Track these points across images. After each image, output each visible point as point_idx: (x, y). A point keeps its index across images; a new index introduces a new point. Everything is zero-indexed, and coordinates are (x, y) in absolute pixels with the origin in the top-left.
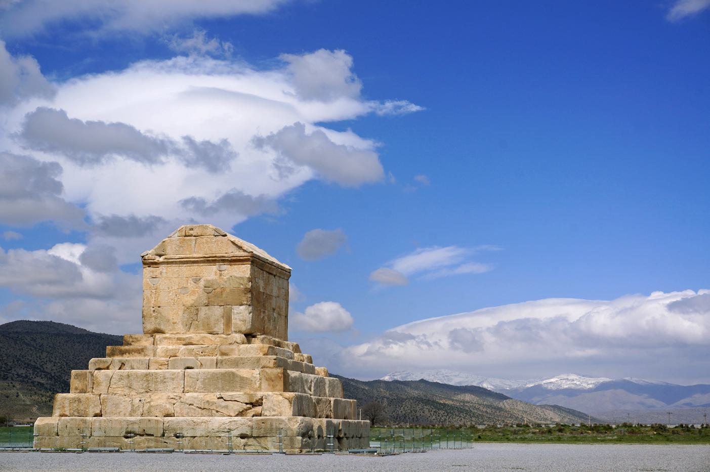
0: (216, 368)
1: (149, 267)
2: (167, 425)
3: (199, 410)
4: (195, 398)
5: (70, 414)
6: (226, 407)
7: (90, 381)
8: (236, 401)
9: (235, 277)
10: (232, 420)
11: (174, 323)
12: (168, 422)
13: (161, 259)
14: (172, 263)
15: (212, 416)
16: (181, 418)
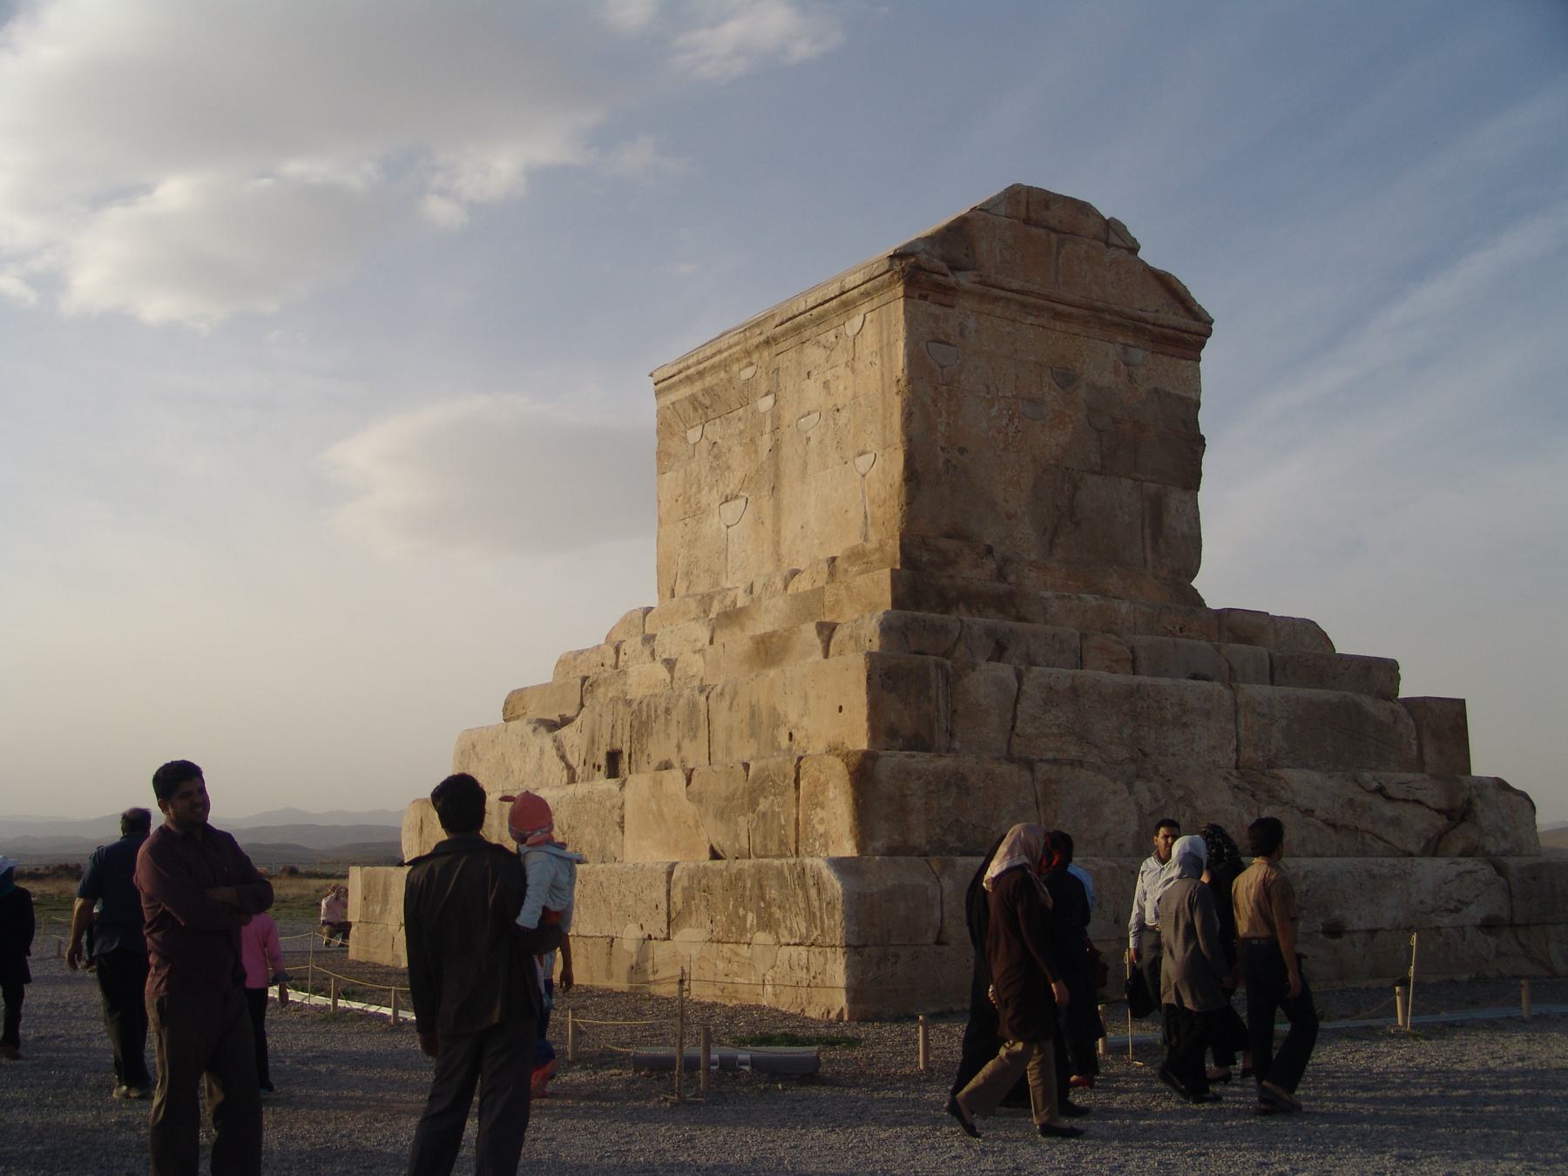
0: (1272, 683)
1: (924, 297)
2: (1304, 888)
3: (1330, 831)
4: (1317, 788)
5: (928, 842)
6: (1396, 822)
7: (942, 703)
8: (1418, 802)
9: (1169, 395)
10: (1461, 868)
11: (1010, 516)
12: (1305, 877)
13: (965, 279)
14: (996, 299)
15: (1365, 854)
16: (1337, 863)
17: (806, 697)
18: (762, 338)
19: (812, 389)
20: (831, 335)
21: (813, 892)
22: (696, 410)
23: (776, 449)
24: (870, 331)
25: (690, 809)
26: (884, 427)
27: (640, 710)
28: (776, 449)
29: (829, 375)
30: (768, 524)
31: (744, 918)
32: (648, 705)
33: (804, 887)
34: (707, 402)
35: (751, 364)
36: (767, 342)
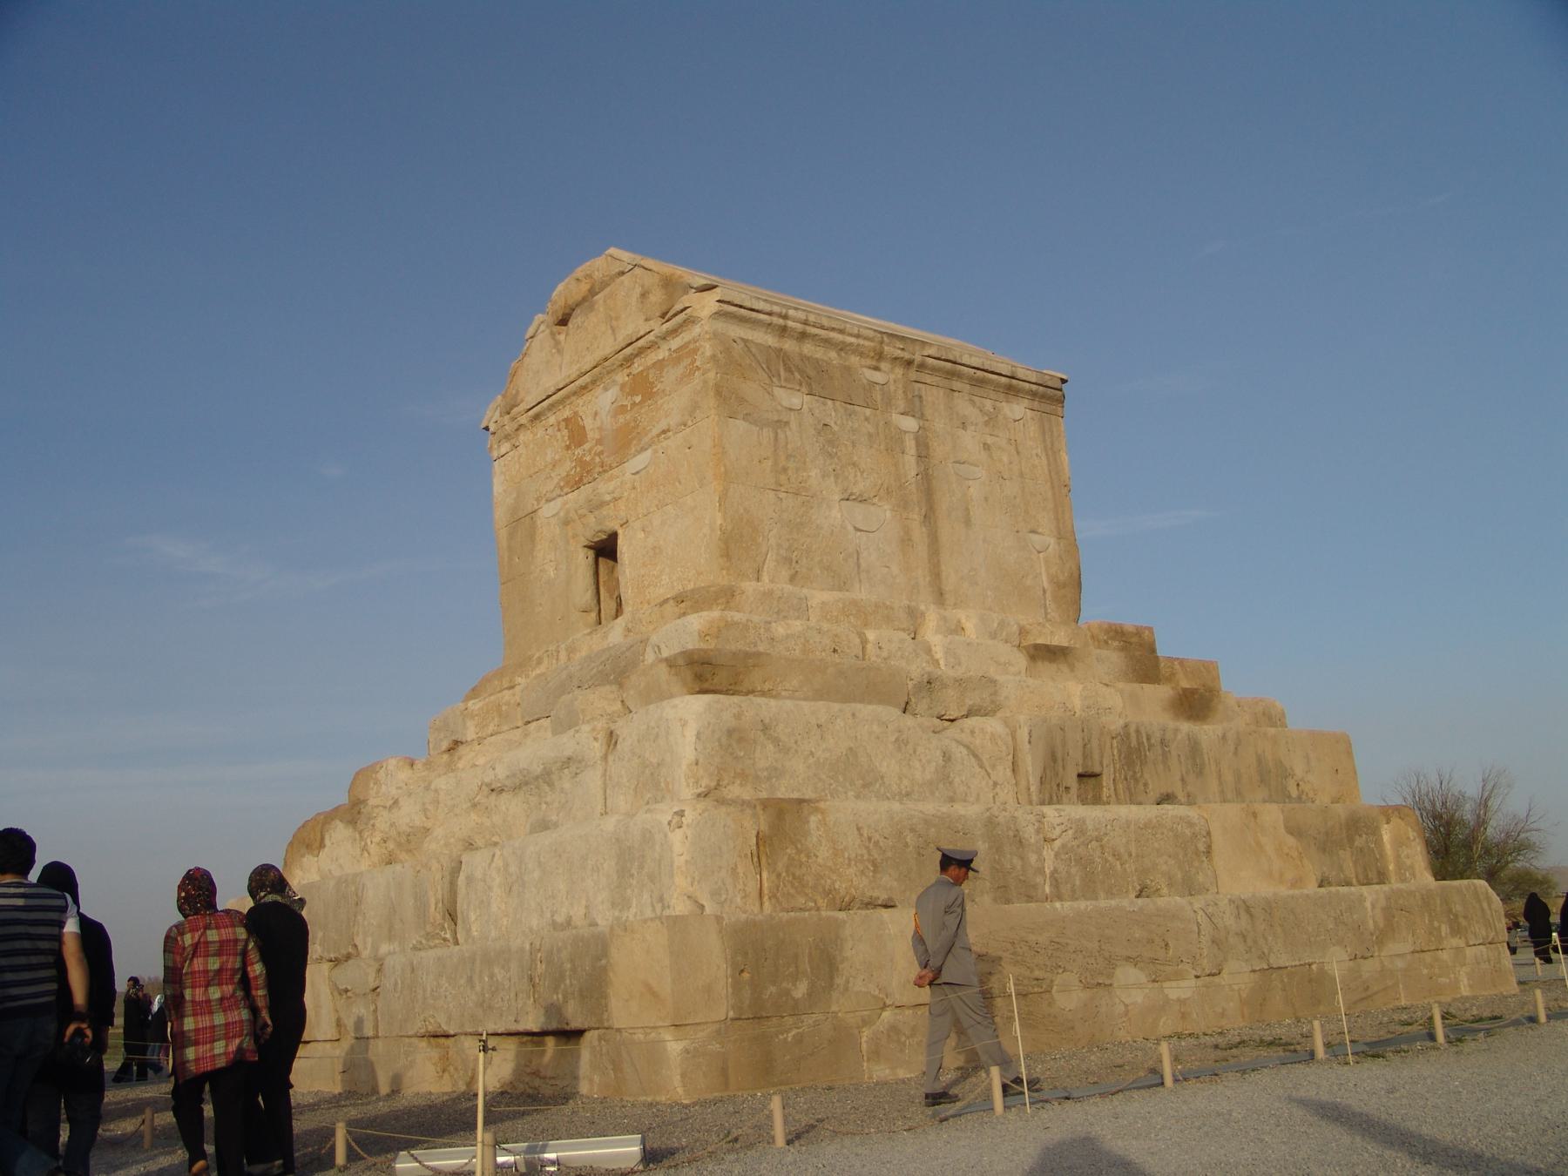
17: (1307, 757)
18: (907, 356)
19: (969, 441)
20: (988, 404)
21: (1485, 905)
22: (788, 370)
23: (926, 477)
24: (1033, 429)
25: (1291, 841)
26: (1057, 519)
27: (1128, 735)
28: (926, 477)
29: (989, 440)
30: (922, 549)
31: (1439, 929)
32: (1138, 731)
33: (1479, 901)
34: (812, 373)
35: (877, 369)
36: (909, 363)
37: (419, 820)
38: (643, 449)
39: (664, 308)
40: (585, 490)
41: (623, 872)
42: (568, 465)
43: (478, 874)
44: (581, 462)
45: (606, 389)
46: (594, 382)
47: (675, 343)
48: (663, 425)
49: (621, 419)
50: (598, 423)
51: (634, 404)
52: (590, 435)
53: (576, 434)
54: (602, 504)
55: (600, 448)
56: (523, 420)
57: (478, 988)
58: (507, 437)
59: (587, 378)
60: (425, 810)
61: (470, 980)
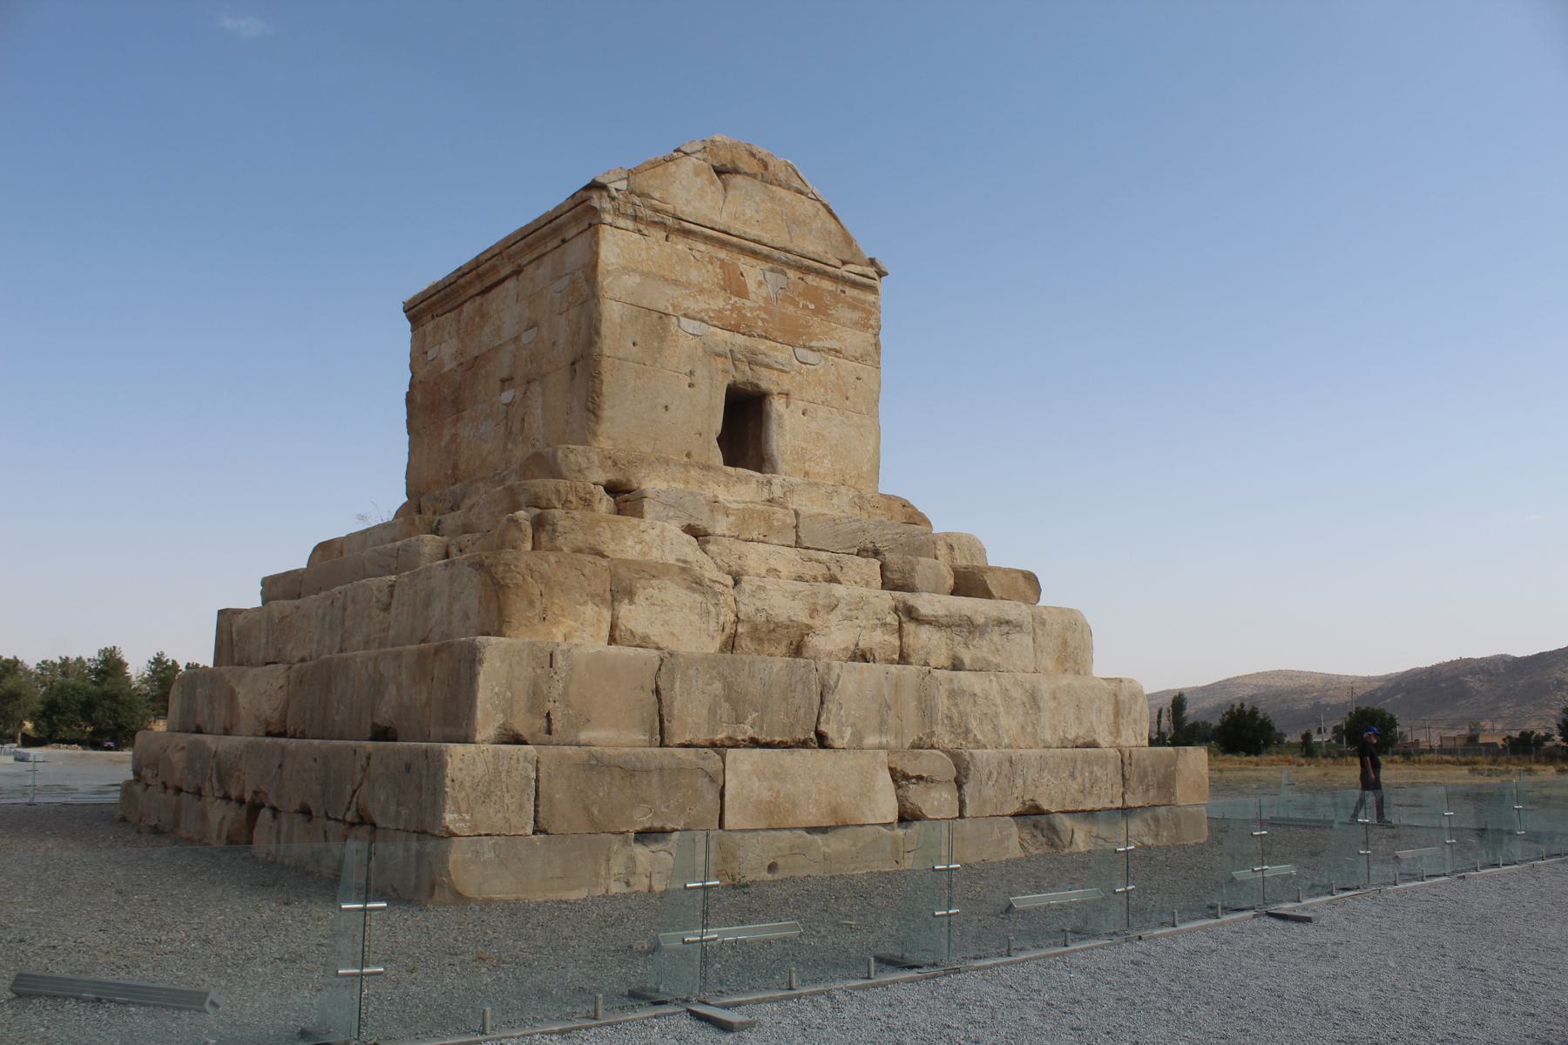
37: (804, 618)
38: (811, 349)
39: (846, 258)
40: (739, 339)
41: (1117, 714)
42: (719, 303)
43: (978, 691)
44: (739, 310)
45: (772, 270)
46: (767, 258)
47: (855, 293)
48: (836, 345)
49: (791, 308)
50: (763, 292)
51: (806, 307)
52: (752, 296)
53: (734, 286)
54: (768, 366)
55: (764, 316)
56: (670, 221)
57: (1079, 780)
58: (635, 218)
59: (765, 250)
60: (813, 612)
61: (1072, 776)
